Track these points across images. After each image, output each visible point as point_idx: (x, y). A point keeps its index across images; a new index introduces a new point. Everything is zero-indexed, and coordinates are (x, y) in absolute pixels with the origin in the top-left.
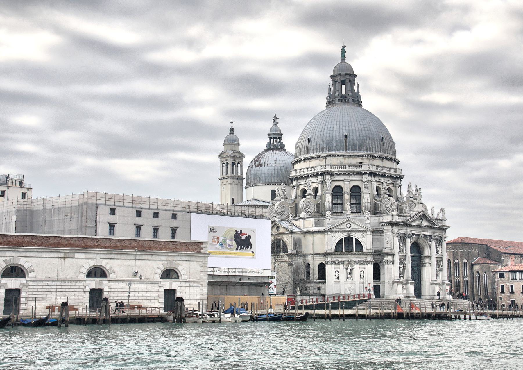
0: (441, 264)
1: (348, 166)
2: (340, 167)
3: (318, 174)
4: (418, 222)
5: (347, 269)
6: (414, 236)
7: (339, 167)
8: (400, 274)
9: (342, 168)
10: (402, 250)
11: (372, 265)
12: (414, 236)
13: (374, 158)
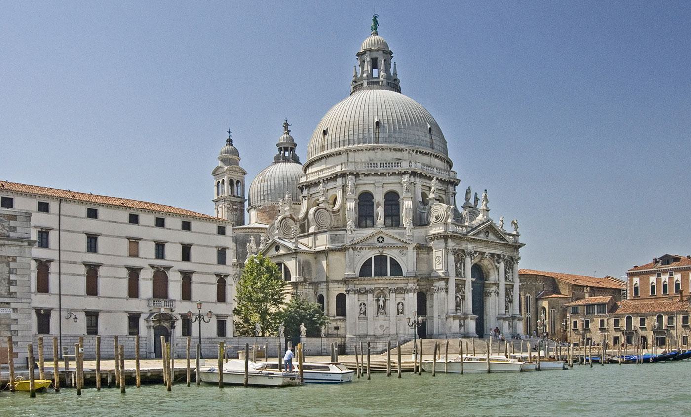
1: (381, 164)
6: (476, 254)
10: (460, 273)
12: (476, 254)
13: (418, 153)
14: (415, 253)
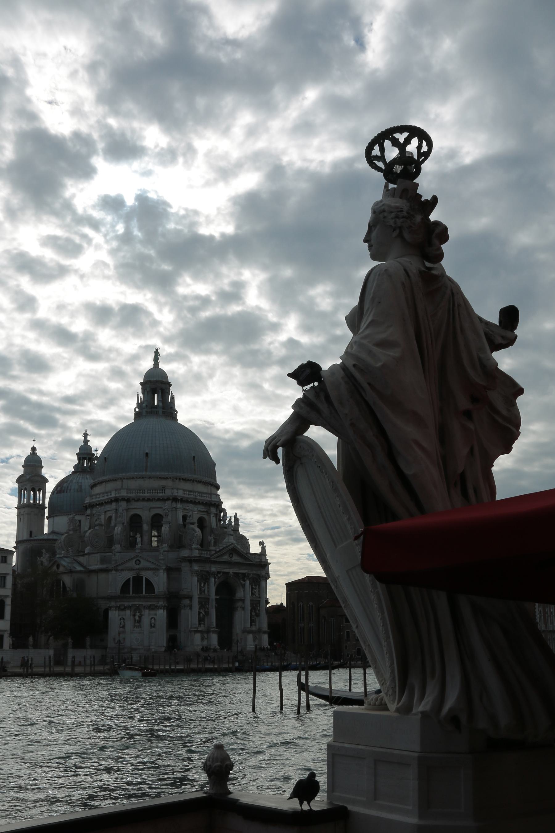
0: (258, 607)
1: (148, 491)
2: (139, 492)
3: (111, 500)
4: (226, 558)
5: (134, 615)
6: (220, 574)
7: (136, 492)
8: (199, 621)
9: (140, 493)
11: (165, 611)
12: (220, 574)
13: (181, 480)
14: (165, 574)
